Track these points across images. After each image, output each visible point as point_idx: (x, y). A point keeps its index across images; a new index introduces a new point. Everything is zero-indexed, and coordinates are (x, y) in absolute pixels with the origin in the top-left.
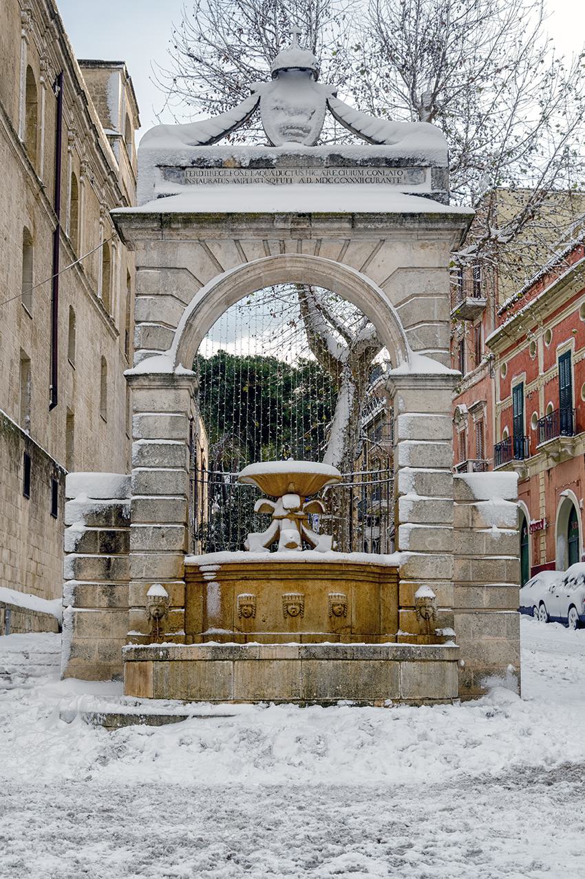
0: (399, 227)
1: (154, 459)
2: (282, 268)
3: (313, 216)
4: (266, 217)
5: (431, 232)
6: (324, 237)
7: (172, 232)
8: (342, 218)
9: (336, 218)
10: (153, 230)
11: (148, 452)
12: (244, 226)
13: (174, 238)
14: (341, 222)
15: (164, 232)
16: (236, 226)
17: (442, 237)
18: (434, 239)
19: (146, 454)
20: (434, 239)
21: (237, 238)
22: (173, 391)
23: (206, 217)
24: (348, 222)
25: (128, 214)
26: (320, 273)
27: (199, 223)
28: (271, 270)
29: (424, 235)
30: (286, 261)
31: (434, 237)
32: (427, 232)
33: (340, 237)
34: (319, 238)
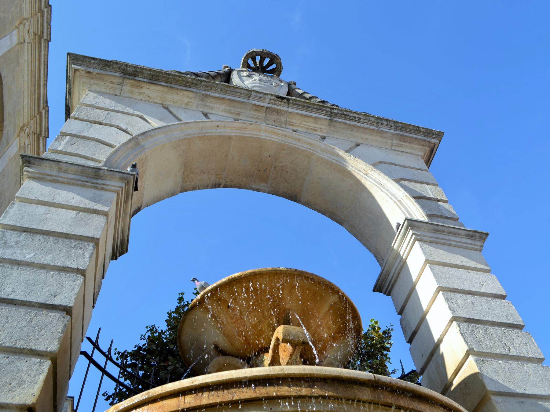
0: (376, 128)
1: (25, 252)
2: (257, 135)
3: (291, 101)
4: (242, 91)
5: (404, 143)
6: (299, 129)
7: (134, 89)
8: (320, 109)
9: (315, 108)
10: (112, 83)
11: (17, 242)
12: (217, 95)
13: (134, 96)
14: (319, 113)
15: (124, 88)
16: (207, 93)
17: (414, 152)
18: (407, 153)
19: (13, 244)
20: (407, 153)
21: (206, 111)
22: (93, 191)
23: (177, 78)
24: (326, 115)
25: (88, 57)
26: (299, 147)
27: (167, 82)
28: (243, 134)
29: (399, 146)
30: (260, 130)
31: (407, 150)
32: (401, 143)
33: (316, 133)
34: (295, 128)
